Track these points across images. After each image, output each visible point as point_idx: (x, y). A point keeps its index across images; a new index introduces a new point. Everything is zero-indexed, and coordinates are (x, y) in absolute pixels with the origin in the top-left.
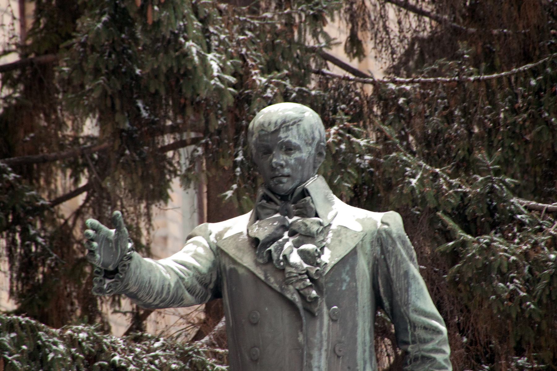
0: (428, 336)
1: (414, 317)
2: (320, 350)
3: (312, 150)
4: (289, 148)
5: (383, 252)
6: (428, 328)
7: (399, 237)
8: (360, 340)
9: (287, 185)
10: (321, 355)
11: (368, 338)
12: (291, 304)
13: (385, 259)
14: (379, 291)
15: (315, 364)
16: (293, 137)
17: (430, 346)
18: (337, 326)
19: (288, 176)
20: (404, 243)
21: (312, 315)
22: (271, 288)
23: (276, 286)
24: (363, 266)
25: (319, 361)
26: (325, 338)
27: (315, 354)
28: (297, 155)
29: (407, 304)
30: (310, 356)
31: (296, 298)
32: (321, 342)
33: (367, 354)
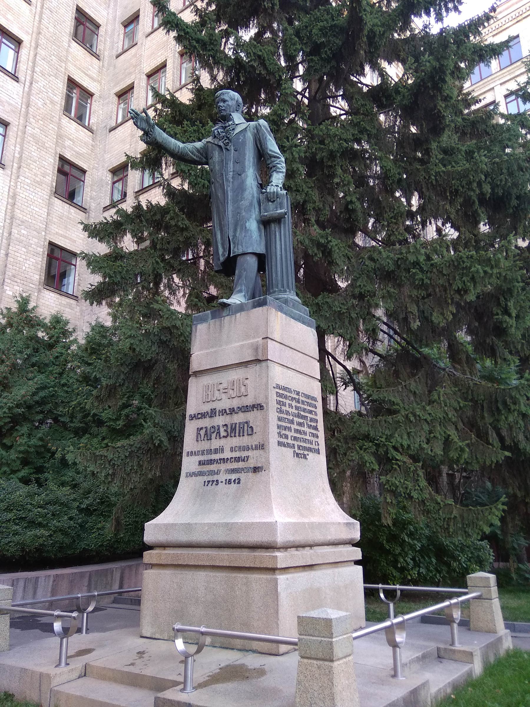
1: (270, 153)
3: (234, 102)
4: (224, 101)
6: (275, 157)
7: (264, 126)
8: (247, 159)
9: (224, 113)
11: (252, 159)
12: (220, 147)
16: (226, 97)
20: (267, 129)
24: (250, 136)
28: (227, 103)
29: (267, 148)
31: (222, 144)
33: (251, 164)
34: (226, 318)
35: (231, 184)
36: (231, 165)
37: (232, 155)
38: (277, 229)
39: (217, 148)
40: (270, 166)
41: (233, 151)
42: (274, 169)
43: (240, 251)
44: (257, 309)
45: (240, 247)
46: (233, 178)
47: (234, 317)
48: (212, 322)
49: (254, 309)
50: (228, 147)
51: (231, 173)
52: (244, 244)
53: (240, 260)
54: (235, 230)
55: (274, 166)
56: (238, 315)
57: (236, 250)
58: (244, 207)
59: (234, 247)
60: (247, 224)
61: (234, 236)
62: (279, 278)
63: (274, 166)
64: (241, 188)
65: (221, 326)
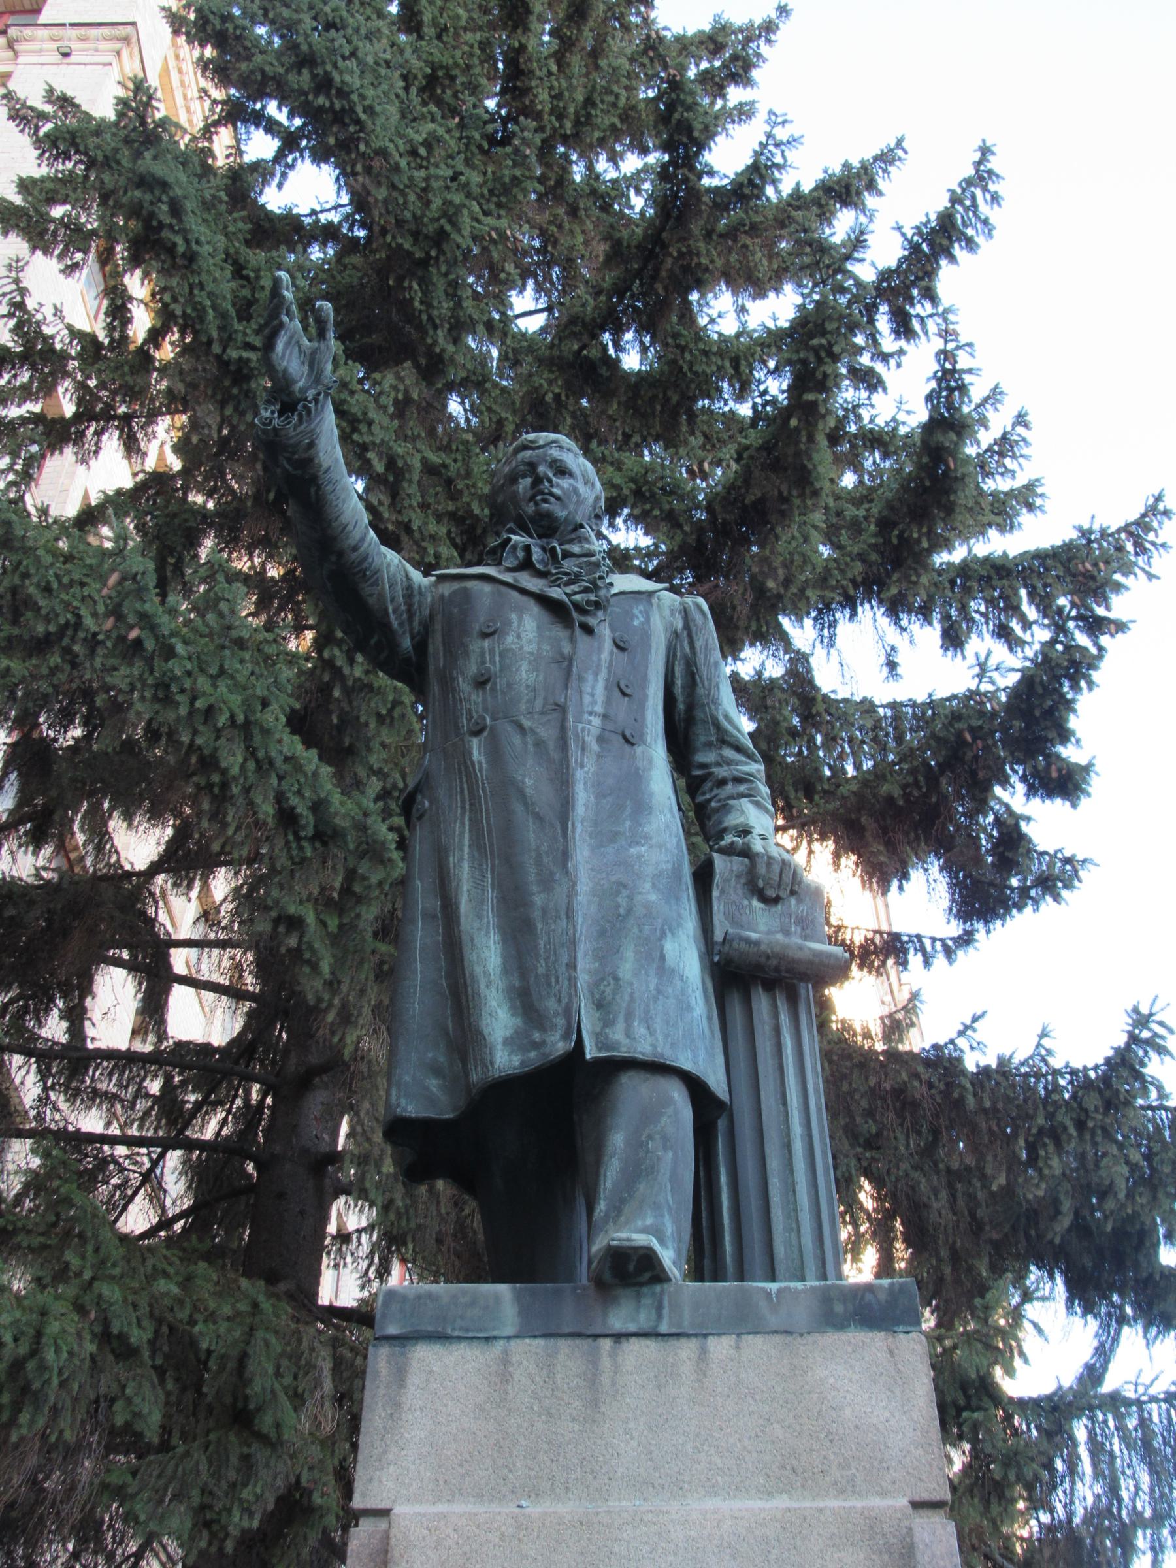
0: (744, 759)
2: (596, 674)
5: (687, 626)
6: (739, 749)
10: (596, 680)
13: (690, 636)
14: (673, 683)
15: (587, 688)
17: (746, 768)
18: (622, 657)
19: (558, 498)
21: (588, 630)
22: (524, 592)
23: (535, 589)
25: (593, 688)
26: (604, 665)
27: (590, 677)
30: (581, 679)
32: (599, 666)
34: (634, 1347)
35: (590, 765)
36: (595, 692)
37: (605, 656)
38: (784, 1018)
39: (534, 608)
40: (722, 772)
41: (608, 644)
42: (742, 788)
43: (643, 1048)
44: (856, 1336)
45: (640, 1030)
46: (601, 740)
47: (687, 1350)
48: (527, 1353)
49: (832, 1338)
50: (591, 621)
51: (596, 721)
52: (658, 1025)
53: (634, 1091)
54: (607, 953)
55: (738, 780)
56: (721, 1347)
57: (617, 1034)
58: (650, 870)
59: (608, 1023)
60: (670, 947)
61: (606, 976)
62: (808, 1241)
63: (738, 780)
64: (627, 794)
65: (593, 1382)
